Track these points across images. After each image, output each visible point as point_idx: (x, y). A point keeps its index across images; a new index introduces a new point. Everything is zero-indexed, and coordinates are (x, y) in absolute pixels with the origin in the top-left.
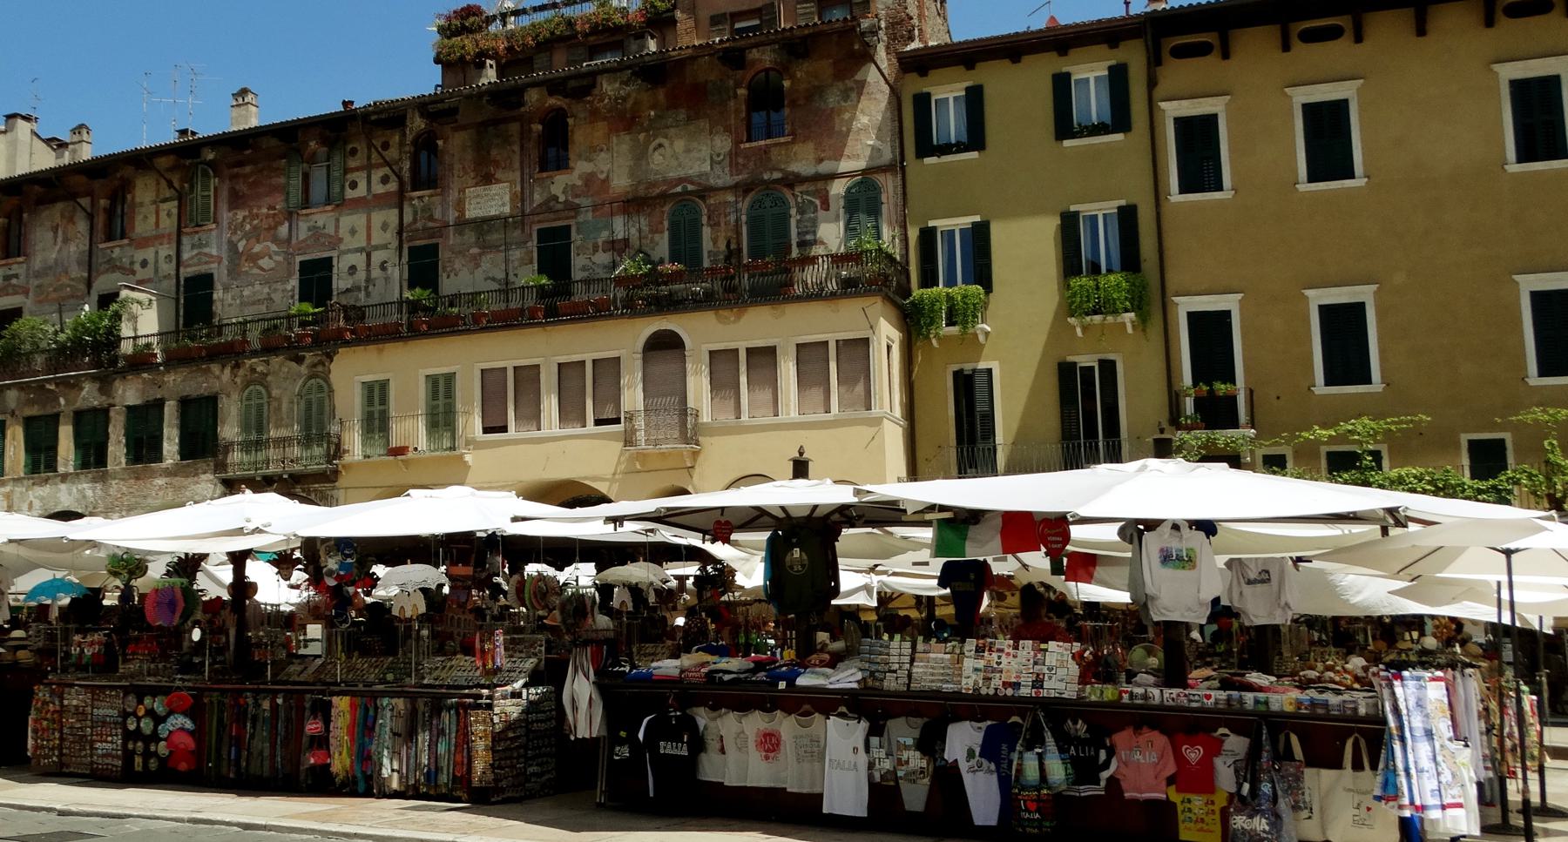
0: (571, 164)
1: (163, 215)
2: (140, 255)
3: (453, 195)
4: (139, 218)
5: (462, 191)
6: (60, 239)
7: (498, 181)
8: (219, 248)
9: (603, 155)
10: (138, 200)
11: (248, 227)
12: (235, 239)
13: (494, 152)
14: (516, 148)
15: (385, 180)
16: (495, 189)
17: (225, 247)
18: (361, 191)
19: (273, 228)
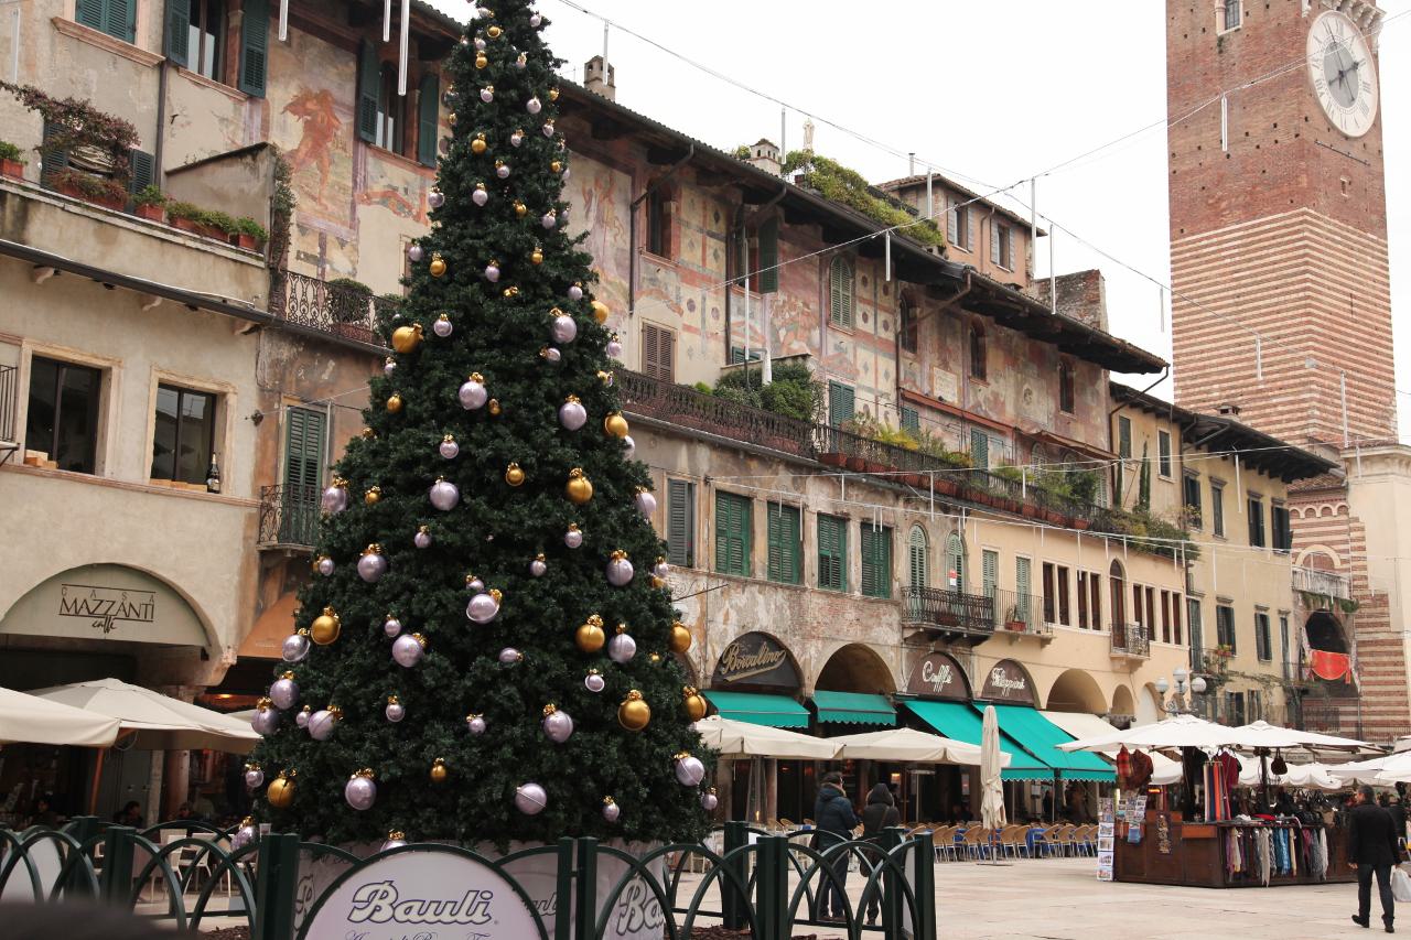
0: (989, 379)
1: (710, 252)
2: (689, 293)
3: (927, 365)
4: (685, 242)
5: (931, 367)
6: (592, 214)
7: (951, 371)
8: (763, 327)
9: (1002, 381)
10: (684, 216)
11: (787, 316)
12: (778, 323)
13: (949, 341)
14: (960, 344)
15: (886, 327)
16: (951, 377)
17: (768, 329)
18: (869, 327)
19: (809, 329)
